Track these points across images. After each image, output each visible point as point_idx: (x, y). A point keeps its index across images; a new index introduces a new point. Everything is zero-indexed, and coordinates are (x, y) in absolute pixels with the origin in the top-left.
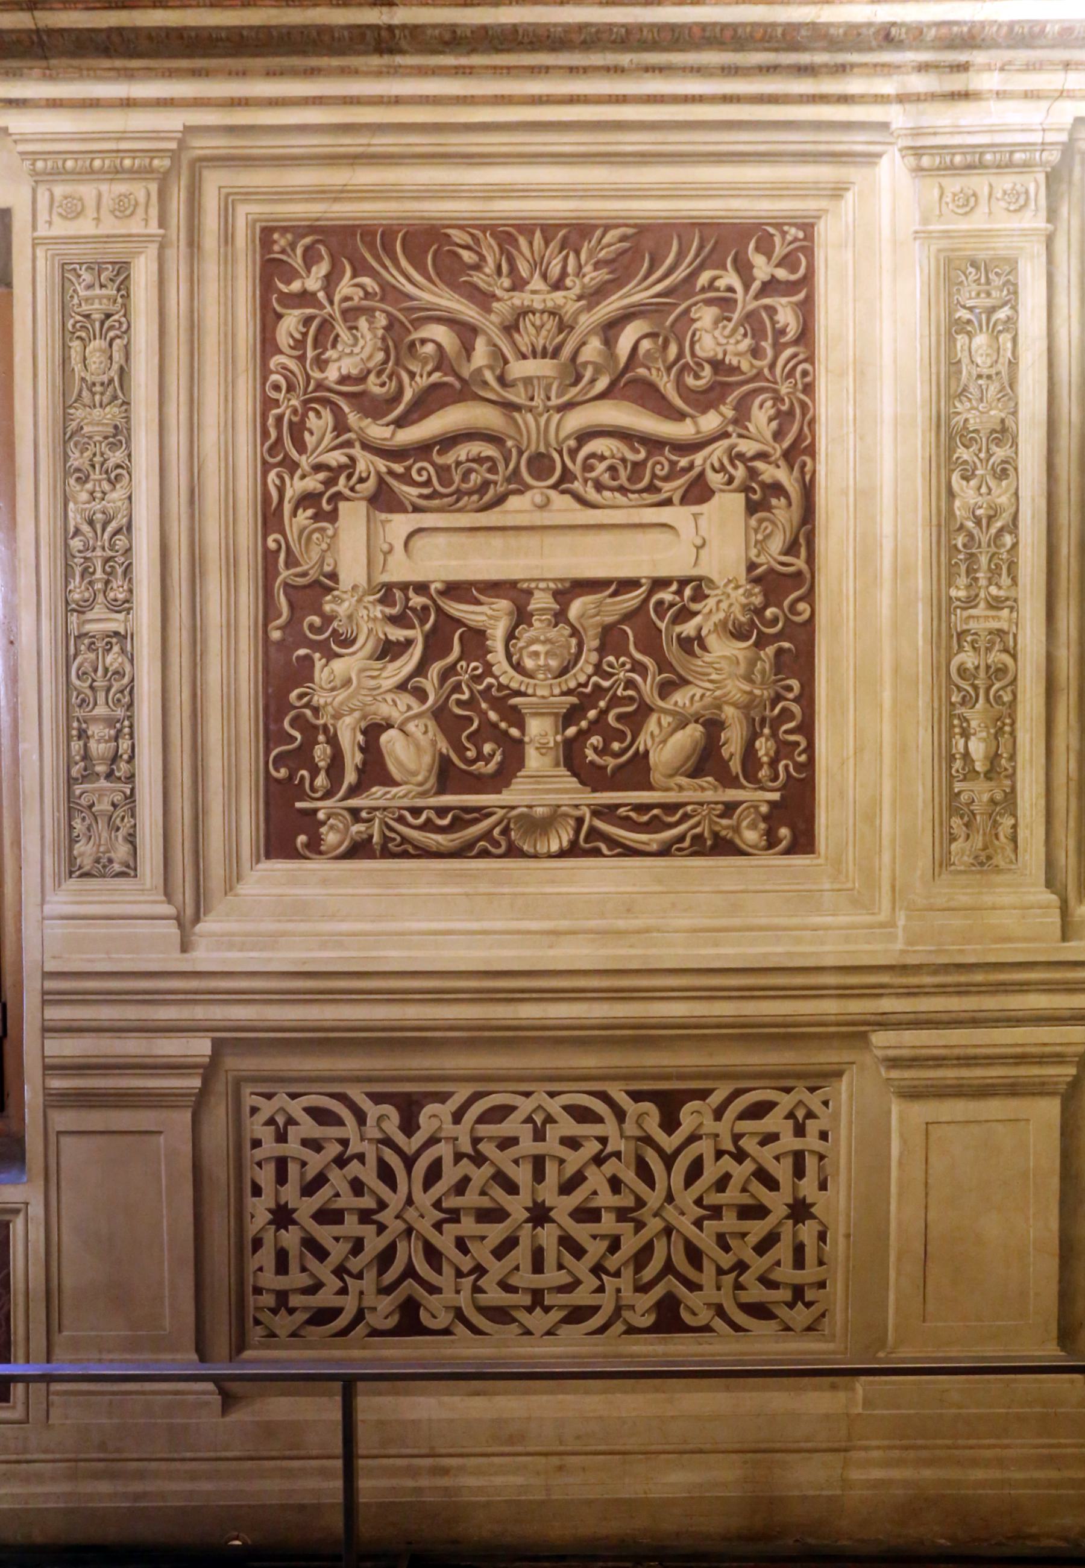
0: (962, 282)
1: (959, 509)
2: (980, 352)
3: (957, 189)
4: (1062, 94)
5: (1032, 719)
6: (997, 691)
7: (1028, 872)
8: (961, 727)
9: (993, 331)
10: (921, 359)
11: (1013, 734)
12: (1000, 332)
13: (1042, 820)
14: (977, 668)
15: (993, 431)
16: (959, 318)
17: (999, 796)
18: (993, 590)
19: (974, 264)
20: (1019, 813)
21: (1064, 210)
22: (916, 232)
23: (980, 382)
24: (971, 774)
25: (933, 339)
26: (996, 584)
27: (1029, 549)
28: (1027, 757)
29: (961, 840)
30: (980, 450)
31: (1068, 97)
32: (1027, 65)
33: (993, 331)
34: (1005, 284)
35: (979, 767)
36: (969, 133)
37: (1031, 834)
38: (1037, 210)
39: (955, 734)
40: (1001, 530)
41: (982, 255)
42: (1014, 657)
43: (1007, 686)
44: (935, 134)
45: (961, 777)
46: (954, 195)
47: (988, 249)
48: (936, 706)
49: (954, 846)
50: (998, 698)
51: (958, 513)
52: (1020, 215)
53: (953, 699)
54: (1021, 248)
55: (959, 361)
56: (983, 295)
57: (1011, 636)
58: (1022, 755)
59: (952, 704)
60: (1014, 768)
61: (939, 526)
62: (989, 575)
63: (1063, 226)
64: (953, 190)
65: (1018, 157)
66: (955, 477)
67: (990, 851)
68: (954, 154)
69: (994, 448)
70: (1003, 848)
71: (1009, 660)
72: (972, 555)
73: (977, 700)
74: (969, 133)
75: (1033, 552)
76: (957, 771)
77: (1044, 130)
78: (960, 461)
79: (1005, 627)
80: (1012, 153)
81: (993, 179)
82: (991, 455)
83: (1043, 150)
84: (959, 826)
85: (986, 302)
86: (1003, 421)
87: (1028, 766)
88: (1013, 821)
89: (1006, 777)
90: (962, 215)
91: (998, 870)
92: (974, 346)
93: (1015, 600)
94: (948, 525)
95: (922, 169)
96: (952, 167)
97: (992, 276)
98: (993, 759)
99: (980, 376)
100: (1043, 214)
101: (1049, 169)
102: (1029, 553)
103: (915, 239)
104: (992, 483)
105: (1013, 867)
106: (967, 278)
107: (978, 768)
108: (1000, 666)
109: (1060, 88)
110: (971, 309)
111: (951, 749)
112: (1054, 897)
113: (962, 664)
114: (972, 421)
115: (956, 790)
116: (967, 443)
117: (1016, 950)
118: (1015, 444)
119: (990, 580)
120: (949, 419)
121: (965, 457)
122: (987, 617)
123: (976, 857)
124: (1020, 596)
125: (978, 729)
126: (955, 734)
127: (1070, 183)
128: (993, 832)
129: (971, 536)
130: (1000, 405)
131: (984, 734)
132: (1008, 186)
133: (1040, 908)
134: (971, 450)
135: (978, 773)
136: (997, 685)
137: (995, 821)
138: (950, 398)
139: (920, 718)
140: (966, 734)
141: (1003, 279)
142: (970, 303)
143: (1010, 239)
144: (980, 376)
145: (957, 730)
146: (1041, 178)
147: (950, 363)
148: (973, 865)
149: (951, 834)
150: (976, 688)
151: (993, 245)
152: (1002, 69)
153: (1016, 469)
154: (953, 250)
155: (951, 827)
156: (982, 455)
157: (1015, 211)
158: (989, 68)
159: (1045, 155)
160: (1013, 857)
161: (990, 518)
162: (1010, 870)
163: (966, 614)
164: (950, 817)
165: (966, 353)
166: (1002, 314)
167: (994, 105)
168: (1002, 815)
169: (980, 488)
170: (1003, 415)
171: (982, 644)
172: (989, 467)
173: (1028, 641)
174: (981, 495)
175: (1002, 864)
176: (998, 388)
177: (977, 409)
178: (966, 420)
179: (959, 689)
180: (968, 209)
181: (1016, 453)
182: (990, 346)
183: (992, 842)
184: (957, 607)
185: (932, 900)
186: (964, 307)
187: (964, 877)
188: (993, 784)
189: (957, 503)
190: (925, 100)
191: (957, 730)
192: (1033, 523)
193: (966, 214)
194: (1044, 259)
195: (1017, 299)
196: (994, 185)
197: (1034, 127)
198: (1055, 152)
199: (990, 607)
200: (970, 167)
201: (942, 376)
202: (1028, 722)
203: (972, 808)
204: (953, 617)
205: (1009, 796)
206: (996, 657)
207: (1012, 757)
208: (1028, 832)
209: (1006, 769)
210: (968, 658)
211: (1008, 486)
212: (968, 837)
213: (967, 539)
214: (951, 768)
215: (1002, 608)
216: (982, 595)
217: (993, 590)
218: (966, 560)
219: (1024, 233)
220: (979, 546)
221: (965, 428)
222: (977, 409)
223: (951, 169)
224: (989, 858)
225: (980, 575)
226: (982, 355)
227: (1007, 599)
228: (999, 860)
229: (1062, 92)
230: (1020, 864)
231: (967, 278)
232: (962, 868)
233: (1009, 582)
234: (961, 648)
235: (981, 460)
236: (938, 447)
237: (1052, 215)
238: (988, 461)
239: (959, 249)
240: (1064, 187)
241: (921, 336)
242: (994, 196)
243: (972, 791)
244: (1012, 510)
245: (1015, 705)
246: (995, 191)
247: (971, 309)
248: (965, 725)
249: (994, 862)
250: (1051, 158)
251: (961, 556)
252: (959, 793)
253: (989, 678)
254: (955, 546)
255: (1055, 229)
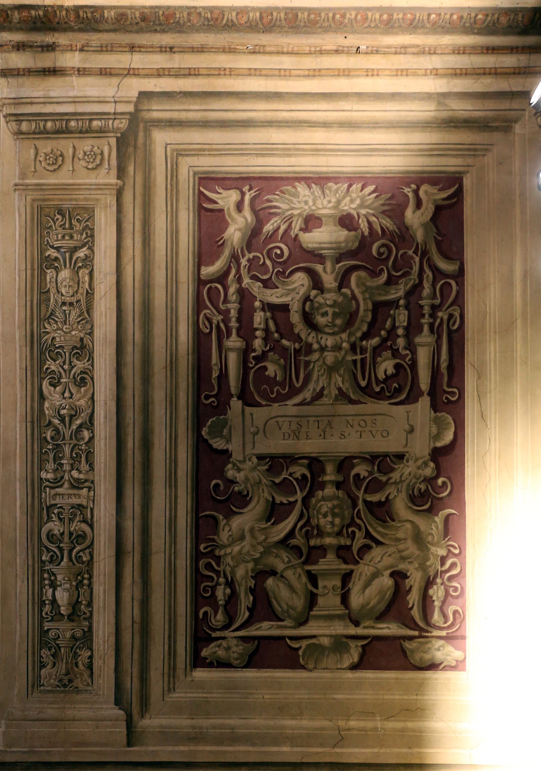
0: (51, 226)
1: (47, 409)
2: (64, 283)
3: (49, 150)
4: (131, 72)
5: (105, 575)
6: (78, 553)
7: (101, 693)
8: (50, 579)
9: (74, 268)
10: (19, 289)
11: (90, 585)
12: (80, 268)
13: (112, 652)
14: (62, 534)
15: (75, 347)
16: (49, 255)
17: (79, 634)
18: (75, 474)
19: (60, 212)
20: (95, 647)
21: (131, 169)
22: (16, 185)
23: (64, 308)
24: (57, 616)
25: (29, 272)
26: (77, 469)
27: (103, 442)
28: (101, 604)
29: (49, 667)
30: (64, 363)
31: (134, 74)
32: (101, 47)
33: (74, 268)
34: (84, 229)
35: (63, 610)
36: (58, 103)
37: (104, 663)
38: (110, 169)
39: (46, 585)
40: (80, 426)
41: (66, 205)
42: (91, 526)
43: (85, 549)
44: (31, 103)
45: (50, 618)
46: (46, 155)
47: (71, 200)
48: (30, 563)
49: (43, 671)
50: (79, 558)
51: (47, 412)
52: (96, 172)
53: (44, 558)
54: (97, 200)
55: (48, 290)
56: (67, 238)
57: (89, 509)
58: (98, 602)
59: (43, 562)
60: (91, 612)
61: (32, 422)
62: (71, 462)
63: (130, 182)
64: (45, 151)
65: (95, 123)
66: (45, 383)
67: (71, 676)
68: (46, 121)
69: (75, 361)
70: (81, 674)
71: (87, 529)
72: (58, 445)
73: (62, 560)
74: (58, 103)
75: (106, 444)
76: (47, 614)
77: (115, 102)
78: (49, 371)
79: (84, 503)
80: (91, 120)
81: (76, 142)
82: (73, 367)
83: (115, 119)
84: (47, 655)
85: (68, 243)
86: (82, 340)
87: (102, 610)
88: (89, 653)
89: (85, 619)
90: (51, 171)
91: (77, 691)
92: (60, 278)
93: (92, 482)
94: (39, 420)
95: (22, 133)
96: (45, 131)
97: (74, 222)
98: (75, 605)
99: (64, 304)
100: (114, 172)
101: (119, 135)
102: (102, 445)
103: (15, 190)
104: (74, 390)
105: (90, 688)
106: (55, 223)
107: (62, 612)
108: (80, 533)
109: (128, 67)
110: (58, 249)
111: (42, 597)
112: (122, 712)
113: (50, 530)
114: (58, 339)
115: (46, 628)
116: (54, 357)
117: (92, 752)
118: (91, 358)
119: (72, 465)
120: (40, 338)
121: (53, 368)
122: (70, 495)
123: (60, 681)
124: (96, 479)
125: (63, 582)
126: (46, 585)
127: (135, 147)
128: (74, 661)
129: (57, 430)
130: (79, 327)
131: (68, 586)
132: (87, 148)
133: (111, 720)
134: (57, 362)
135: (62, 615)
136: (78, 548)
137: (76, 653)
138: (40, 320)
139: (18, 573)
140: (54, 586)
141: (83, 224)
142: (57, 244)
143: (89, 193)
144: (64, 304)
145: (47, 582)
146: (113, 141)
147: (41, 292)
148: (58, 686)
149: (41, 662)
150: (61, 550)
151: (75, 196)
152: (82, 50)
153: (92, 378)
154: (45, 200)
155: (41, 657)
156: (66, 367)
157: (93, 169)
158: (71, 49)
159: (116, 122)
160: (90, 682)
161: (71, 416)
162: (86, 691)
163: (53, 492)
164: (41, 649)
165: (54, 285)
166: (82, 253)
167: (75, 80)
168: (81, 649)
169: (63, 394)
170: (82, 335)
171: (66, 516)
172: (71, 377)
173: (102, 513)
174: (64, 398)
175: (81, 686)
176: (78, 313)
177: (62, 330)
178: (54, 338)
179: (48, 550)
180: (56, 167)
181: (93, 366)
182: (72, 279)
183: (72, 668)
184: (46, 486)
185: (26, 713)
186: (52, 247)
187: (51, 695)
188: (74, 624)
189: (46, 405)
190: (24, 75)
191: (47, 582)
192: (105, 422)
193: (55, 170)
194: (114, 208)
195: (93, 241)
196: (77, 147)
197: (107, 99)
198: (124, 121)
199: (73, 487)
200: (58, 132)
201: (35, 302)
202: (102, 577)
203: (57, 642)
204: (43, 494)
205: (87, 634)
206: (77, 526)
207: (90, 604)
208: (101, 662)
209: (85, 613)
210: (55, 526)
211: (86, 392)
212: (54, 664)
213: (54, 432)
214: (42, 611)
215: (82, 488)
216: (66, 477)
217: (75, 474)
218: (53, 449)
219: (100, 187)
220: (64, 439)
221: (53, 344)
222: (62, 330)
223: (44, 133)
224: (70, 681)
225: (64, 461)
226: (65, 286)
227: (86, 481)
228: (77, 683)
229: (129, 70)
230: (95, 687)
231: (55, 223)
232: (50, 688)
233: (87, 467)
234: (49, 519)
235: (65, 371)
236: (32, 359)
237: (121, 172)
238: (70, 371)
239: (49, 200)
240: (131, 149)
241: (19, 269)
242: (76, 156)
243: (58, 629)
244: (89, 411)
245: (93, 563)
246: (77, 153)
247: (58, 249)
248: (53, 578)
249: (75, 684)
250: (121, 126)
251: (50, 447)
252: (48, 630)
253: (72, 542)
254: (45, 438)
255: (124, 185)
